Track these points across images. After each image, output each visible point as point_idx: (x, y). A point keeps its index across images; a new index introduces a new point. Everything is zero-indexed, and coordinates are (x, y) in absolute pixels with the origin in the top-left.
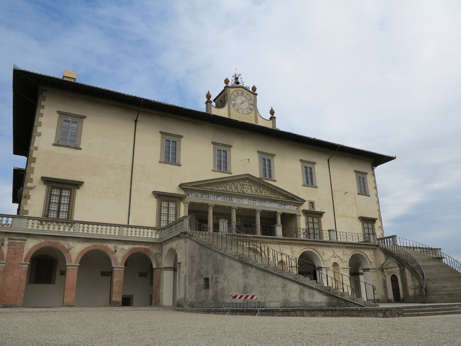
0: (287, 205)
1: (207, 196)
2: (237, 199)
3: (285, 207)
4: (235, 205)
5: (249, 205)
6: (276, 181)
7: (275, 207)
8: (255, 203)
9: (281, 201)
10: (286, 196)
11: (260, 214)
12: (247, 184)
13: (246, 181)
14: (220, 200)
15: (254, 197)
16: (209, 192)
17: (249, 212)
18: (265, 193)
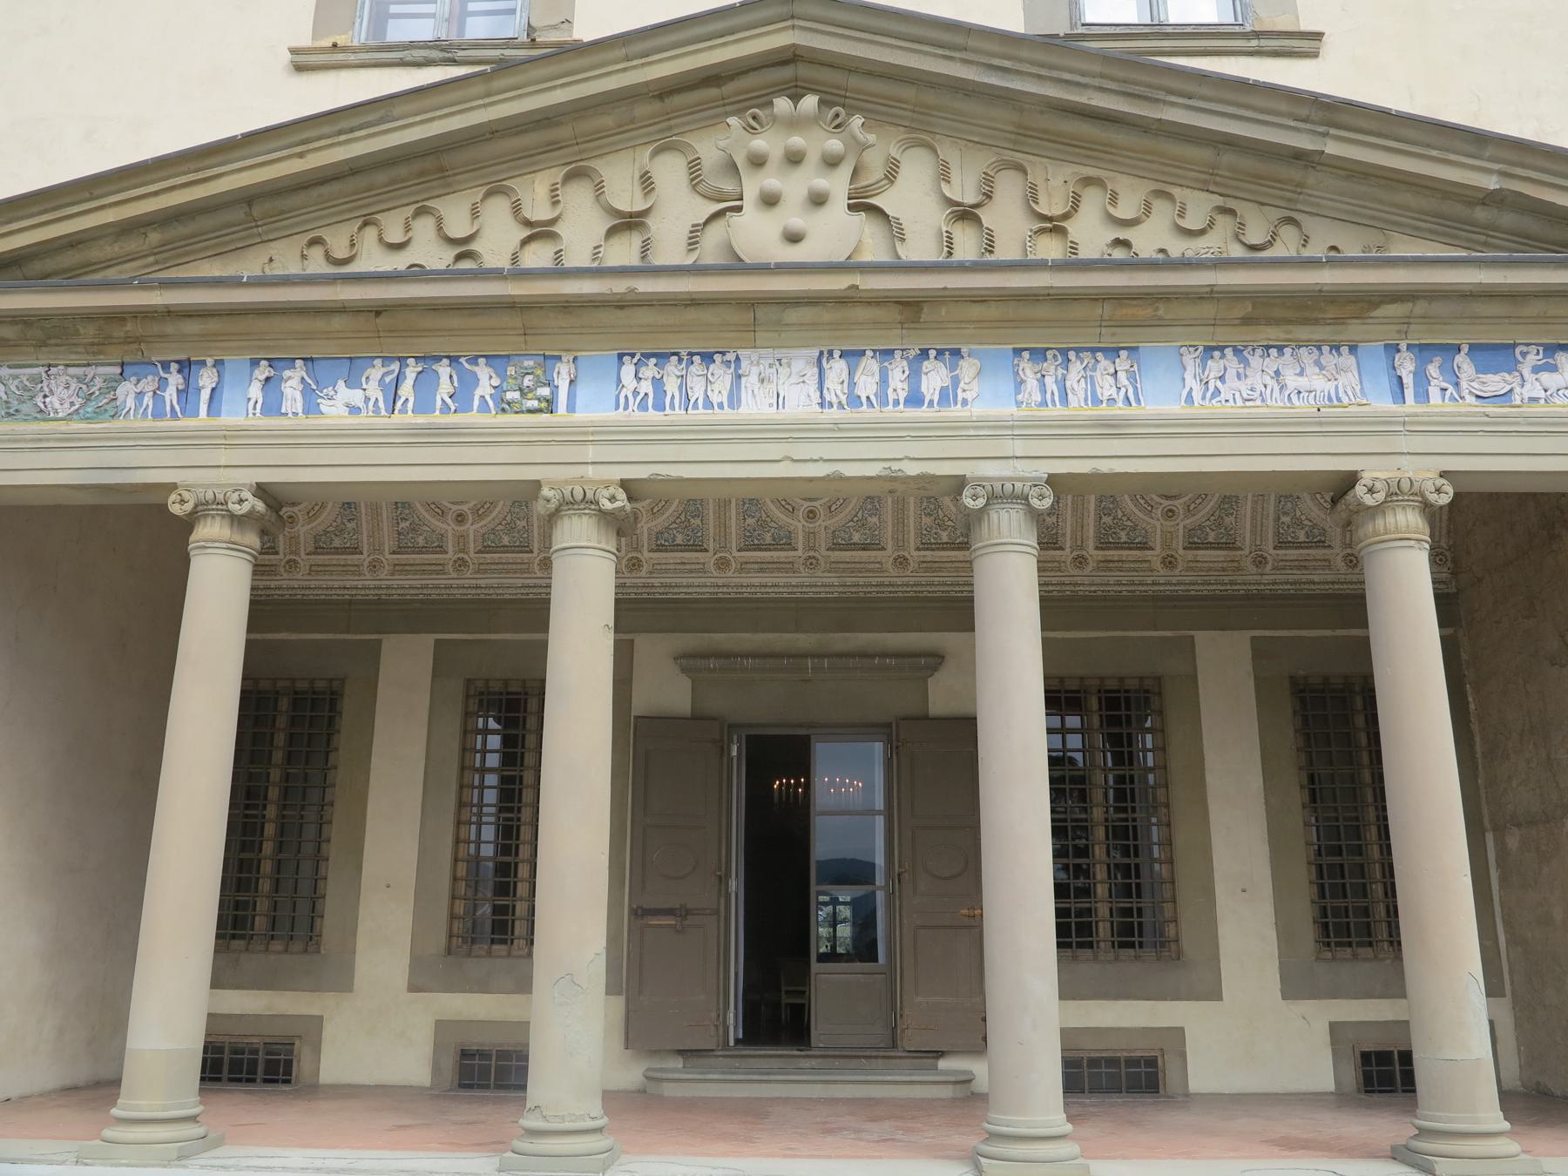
0: (1533, 358)
1: (170, 394)
2: (628, 370)
3: (1495, 383)
4: (591, 453)
5: (837, 426)
6: (1305, 45)
7: (1303, 406)
8: (946, 397)
9: (1420, 307)
10: (1508, 219)
11: (1048, 541)
12: (797, 141)
13: (782, 104)
14: (354, 410)
15: (911, 308)
16: (193, 327)
17: (1102, 545)
18: (1123, 234)
